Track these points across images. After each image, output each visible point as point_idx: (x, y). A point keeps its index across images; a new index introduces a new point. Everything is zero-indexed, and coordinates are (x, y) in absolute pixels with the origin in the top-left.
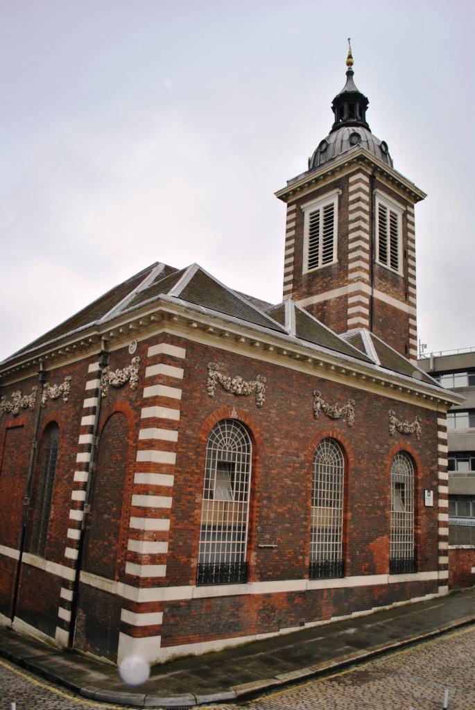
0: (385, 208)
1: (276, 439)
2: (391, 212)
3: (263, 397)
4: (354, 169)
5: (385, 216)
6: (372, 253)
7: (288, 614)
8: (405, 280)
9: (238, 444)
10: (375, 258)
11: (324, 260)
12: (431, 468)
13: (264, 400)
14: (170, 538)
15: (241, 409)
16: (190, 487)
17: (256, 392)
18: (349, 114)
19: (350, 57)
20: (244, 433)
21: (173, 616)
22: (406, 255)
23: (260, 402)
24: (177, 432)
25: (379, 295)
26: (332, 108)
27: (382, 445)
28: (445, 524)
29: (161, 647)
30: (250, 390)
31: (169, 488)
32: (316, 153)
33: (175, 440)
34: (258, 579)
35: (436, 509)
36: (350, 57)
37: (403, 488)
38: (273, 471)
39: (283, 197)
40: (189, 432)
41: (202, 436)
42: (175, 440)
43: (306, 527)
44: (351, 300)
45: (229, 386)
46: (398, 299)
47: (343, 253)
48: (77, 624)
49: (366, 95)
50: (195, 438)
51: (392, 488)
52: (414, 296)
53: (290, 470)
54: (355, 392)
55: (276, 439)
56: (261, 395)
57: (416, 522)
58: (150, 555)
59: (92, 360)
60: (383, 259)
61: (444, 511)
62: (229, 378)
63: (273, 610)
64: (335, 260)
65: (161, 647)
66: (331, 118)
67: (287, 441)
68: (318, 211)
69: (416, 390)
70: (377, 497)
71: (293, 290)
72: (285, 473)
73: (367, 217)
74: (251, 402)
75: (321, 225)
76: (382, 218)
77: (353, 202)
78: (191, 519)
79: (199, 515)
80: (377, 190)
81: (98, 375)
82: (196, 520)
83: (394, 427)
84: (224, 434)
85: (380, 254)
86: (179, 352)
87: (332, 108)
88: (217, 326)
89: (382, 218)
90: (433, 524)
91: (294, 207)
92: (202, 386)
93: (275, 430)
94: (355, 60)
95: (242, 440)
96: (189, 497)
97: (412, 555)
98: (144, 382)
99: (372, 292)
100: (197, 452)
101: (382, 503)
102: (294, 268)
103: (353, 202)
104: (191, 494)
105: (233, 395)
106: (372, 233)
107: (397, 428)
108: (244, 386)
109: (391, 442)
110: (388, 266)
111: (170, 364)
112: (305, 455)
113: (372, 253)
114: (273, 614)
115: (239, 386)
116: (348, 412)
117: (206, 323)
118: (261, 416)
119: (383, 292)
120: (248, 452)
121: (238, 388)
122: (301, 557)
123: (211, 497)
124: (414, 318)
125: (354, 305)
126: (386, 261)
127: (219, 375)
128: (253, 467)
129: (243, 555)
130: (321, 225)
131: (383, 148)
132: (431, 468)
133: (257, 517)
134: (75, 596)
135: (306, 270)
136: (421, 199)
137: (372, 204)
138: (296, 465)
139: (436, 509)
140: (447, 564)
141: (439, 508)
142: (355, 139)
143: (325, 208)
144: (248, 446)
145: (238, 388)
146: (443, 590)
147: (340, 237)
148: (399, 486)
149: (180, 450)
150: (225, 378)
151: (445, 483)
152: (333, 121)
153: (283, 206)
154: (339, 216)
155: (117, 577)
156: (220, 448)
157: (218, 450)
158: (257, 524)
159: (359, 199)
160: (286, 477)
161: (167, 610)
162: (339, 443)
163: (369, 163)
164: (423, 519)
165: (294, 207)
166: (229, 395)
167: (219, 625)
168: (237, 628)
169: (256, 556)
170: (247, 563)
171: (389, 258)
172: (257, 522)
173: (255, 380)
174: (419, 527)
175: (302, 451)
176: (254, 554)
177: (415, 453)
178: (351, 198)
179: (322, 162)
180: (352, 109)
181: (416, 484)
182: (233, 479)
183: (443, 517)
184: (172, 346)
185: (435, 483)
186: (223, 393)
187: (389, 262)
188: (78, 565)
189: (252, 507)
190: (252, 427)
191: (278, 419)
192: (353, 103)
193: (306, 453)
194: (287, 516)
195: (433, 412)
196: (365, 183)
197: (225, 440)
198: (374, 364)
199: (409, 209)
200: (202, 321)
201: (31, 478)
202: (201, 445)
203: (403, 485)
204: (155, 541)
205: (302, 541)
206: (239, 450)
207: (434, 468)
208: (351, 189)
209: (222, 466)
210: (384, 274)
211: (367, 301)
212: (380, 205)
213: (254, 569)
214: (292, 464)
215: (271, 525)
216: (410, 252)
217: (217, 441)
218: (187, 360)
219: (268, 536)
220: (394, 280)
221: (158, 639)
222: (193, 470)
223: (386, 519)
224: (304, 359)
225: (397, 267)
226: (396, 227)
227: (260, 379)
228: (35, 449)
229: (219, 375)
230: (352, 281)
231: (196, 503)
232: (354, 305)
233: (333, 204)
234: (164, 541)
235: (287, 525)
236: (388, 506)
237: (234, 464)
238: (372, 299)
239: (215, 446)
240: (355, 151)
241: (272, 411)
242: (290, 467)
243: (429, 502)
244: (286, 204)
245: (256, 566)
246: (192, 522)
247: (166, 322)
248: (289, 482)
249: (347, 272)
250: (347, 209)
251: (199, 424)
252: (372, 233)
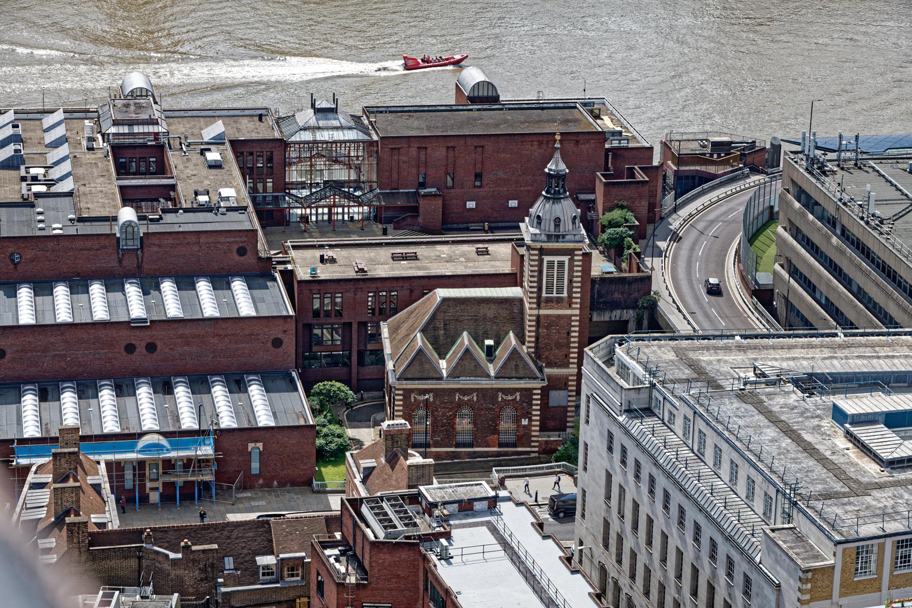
25: (543, 312)
27: (493, 405)
35: (530, 425)
60: (549, 289)
86: (401, 392)
107: (502, 398)
187: (555, 292)
210: (549, 300)
211: (534, 318)
220: (559, 300)
238: (538, 316)
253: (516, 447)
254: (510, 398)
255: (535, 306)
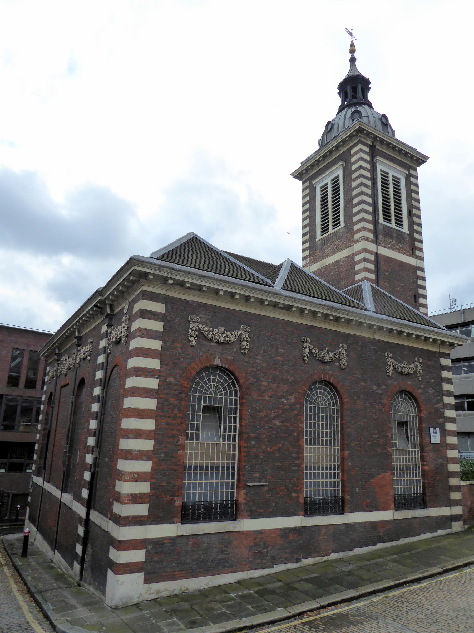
0: (388, 174)
1: (263, 383)
2: (393, 176)
3: (247, 345)
4: (355, 142)
5: (388, 181)
6: (375, 214)
7: (283, 551)
8: (411, 236)
9: (225, 389)
10: (378, 219)
11: (334, 226)
12: (436, 406)
13: (248, 347)
14: (152, 478)
15: (224, 356)
16: (173, 430)
17: (240, 340)
18: (353, 96)
19: (352, 45)
20: (230, 378)
21: (156, 553)
22: (410, 214)
23: (245, 349)
24: (158, 380)
25: (384, 251)
26: (338, 93)
27: (379, 386)
28: (454, 461)
29: (144, 584)
30: (233, 339)
31: (150, 431)
32: (323, 134)
33: (156, 387)
34: (249, 516)
36: (352, 45)
37: (407, 426)
38: (261, 414)
39: (298, 175)
40: (170, 380)
41: (184, 382)
42: (156, 387)
43: (299, 465)
44: (357, 258)
45: (210, 336)
46: (404, 253)
47: (349, 216)
48: (87, 558)
49: (367, 76)
50: (176, 385)
51: (394, 426)
52: (421, 250)
53: (279, 412)
54: (347, 337)
55: (263, 383)
56: (245, 343)
57: (423, 458)
58: (131, 495)
59: (102, 323)
61: (453, 447)
62: (211, 329)
63: (265, 546)
64: (342, 224)
65: (144, 584)
66: (338, 101)
67: (276, 385)
68: (327, 184)
69: (412, 332)
70: (377, 436)
71: (310, 255)
72: (274, 414)
73: (369, 183)
74: (235, 349)
75: (330, 196)
76: (385, 183)
77: (355, 171)
78: (173, 460)
79: (184, 457)
80: (378, 158)
81: (107, 334)
82: (180, 460)
83: (391, 368)
84: (209, 381)
85: (384, 214)
86: (159, 307)
87: (338, 93)
88: (193, 281)
89: (385, 183)
90: (441, 460)
91: (307, 184)
92: (183, 336)
93: (262, 375)
94: (356, 47)
95: (229, 385)
96: (172, 440)
97: (420, 491)
98: (130, 336)
99: (377, 249)
100: (179, 397)
101: (382, 441)
102: (310, 237)
103: (355, 171)
104: (174, 436)
105: (216, 344)
106: (374, 196)
107: (394, 369)
108: (227, 335)
109: (389, 382)
110: (393, 225)
111: (149, 319)
112: (295, 397)
113: (375, 214)
114: (266, 550)
115: (221, 335)
116: (340, 356)
117: (181, 279)
118: (246, 362)
119: (389, 248)
120: (236, 395)
121: (220, 337)
122: (294, 495)
123: (198, 439)
124: (423, 270)
125: (360, 262)
126: (390, 220)
127: (201, 326)
128: (240, 410)
129: (232, 493)
130: (330, 196)
131: (384, 120)
132: (436, 406)
133: (245, 456)
134: (87, 532)
135: (319, 236)
136: (423, 162)
137: (373, 170)
138: (285, 407)
139: (444, 446)
140: (460, 500)
141: (447, 445)
142: (356, 115)
143: (332, 180)
144: (236, 391)
145: (220, 337)
146: (457, 526)
147: (345, 203)
148: (402, 424)
149: (161, 396)
150: (206, 329)
151: (452, 420)
152: (340, 103)
153: (299, 184)
154: (344, 185)
155: (109, 516)
156: (205, 393)
157: (203, 395)
158: (245, 463)
159: (361, 167)
160: (275, 418)
161: (150, 547)
162: (327, 383)
163: (368, 134)
164: (430, 455)
165: (307, 184)
166: (212, 344)
167: (207, 562)
168: (227, 564)
169: (246, 494)
170: (236, 501)
171: (393, 218)
172: (245, 461)
173: (239, 330)
174: (425, 463)
175: (291, 394)
176: (243, 492)
177: (417, 392)
178: (353, 168)
179: (328, 141)
180: (354, 90)
181: (420, 422)
182: (220, 422)
183: (452, 454)
184: (151, 302)
185: (441, 421)
186: (205, 342)
188: (89, 505)
189: (239, 447)
190: (237, 373)
191: (264, 365)
192: (355, 85)
193: (296, 396)
194: (277, 455)
195: (435, 352)
196: (366, 153)
197: (210, 385)
198: (367, 310)
199: (412, 172)
200: (177, 278)
201: (69, 428)
202: (183, 391)
203: (406, 423)
204: (136, 481)
205: (295, 479)
206: (226, 394)
207: (440, 405)
208: (353, 159)
209: (207, 409)
210: (388, 232)
211: (372, 257)
212: (381, 171)
213: (243, 507)
214: (281, 406)
215: (260, 464)
216: (414, 211)
217: (202, 387)
218: (167, 314)
219: (257, 475)
220: (400, 235)
221: (141, 575)
222: (176, 414)
223: (388, 456)
224: (288, 308)
225: (402, 225)
226: (399, 190)
227: (243, 328)
228: (72, 403)
229: (201, 326)
230: (357, 241)
231: (179, 445)
232: (360, 262)
233: (338, 176)
234: (145, 481)
235: (277, 464)
236: (389, 443)
237: (221, 407)
238: (377, 255)
239: (200, 392)
240: (356, 125)
241: (257, 357)
242: (279, 409)
243: (435, 438)
244: (301, 182)
245: (245, 504)
246: (176, 463)
247: (142, 280)
248: (278, 423)
249: (353, 233)
250: (351, 177)
251: (181, 372)
252: (374, 196)
253: (424, 505)
254: (408, 368)
255: (371, 236)
